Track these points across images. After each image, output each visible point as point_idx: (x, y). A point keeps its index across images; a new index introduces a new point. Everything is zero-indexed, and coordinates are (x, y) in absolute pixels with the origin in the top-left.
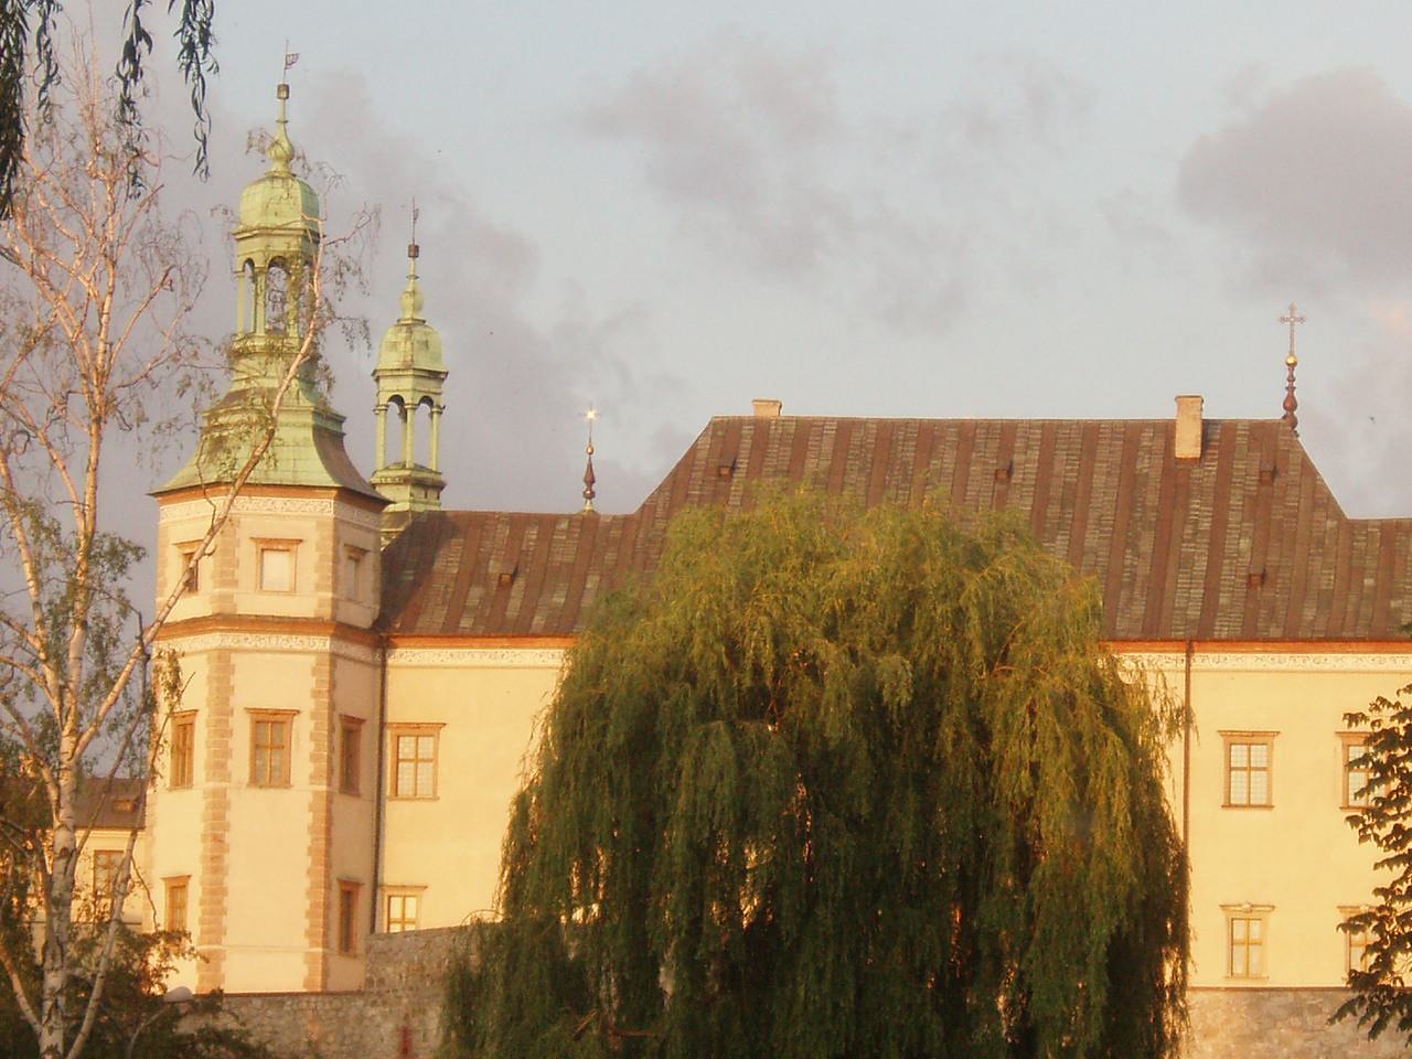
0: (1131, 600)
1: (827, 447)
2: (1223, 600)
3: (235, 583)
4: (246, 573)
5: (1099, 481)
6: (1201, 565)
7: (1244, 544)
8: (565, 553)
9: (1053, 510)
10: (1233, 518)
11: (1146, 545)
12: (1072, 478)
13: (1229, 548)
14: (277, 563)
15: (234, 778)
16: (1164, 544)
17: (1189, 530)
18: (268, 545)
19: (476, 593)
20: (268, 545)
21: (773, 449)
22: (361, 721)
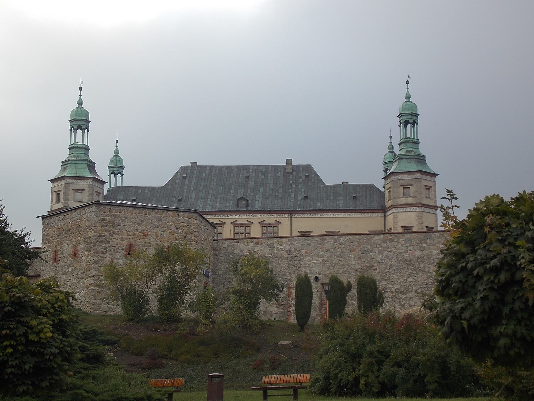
1: (207, 172)
3: (68, 200)
4: (71, 197)
5: (269, 178)
7: (303, 190)
10: (300, 185)
11: (280, 191)
12: (263, 177)
14: (79, 195)
17: (290, 188)
18: (77, 191)
20: (77, 191)
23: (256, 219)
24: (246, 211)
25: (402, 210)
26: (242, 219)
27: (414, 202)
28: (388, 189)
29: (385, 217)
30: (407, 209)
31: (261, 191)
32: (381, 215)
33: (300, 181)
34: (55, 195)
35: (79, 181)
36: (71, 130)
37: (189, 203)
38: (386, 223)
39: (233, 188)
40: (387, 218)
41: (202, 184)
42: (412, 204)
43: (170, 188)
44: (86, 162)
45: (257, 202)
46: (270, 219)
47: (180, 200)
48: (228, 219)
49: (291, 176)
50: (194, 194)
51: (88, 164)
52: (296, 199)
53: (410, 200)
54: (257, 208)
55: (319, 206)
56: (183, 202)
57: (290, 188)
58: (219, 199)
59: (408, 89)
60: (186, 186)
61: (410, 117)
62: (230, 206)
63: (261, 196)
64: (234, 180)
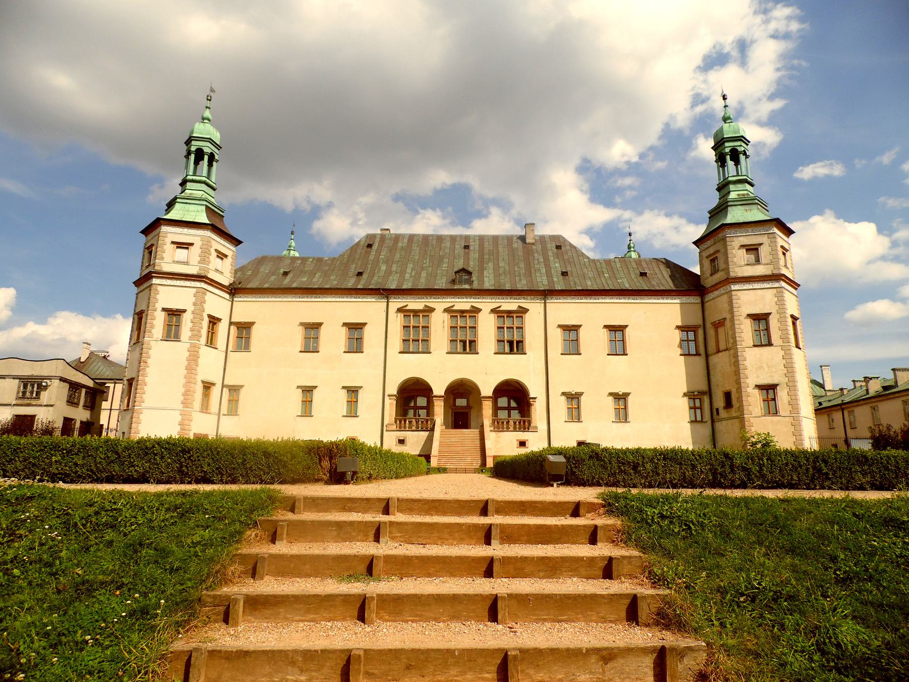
0: (520, 280)
1: (406, 241)
2: (555, 279)
5: (501, 249)
6: (544, 271)
7: (557, 265)
8: (309, 266)
9: (486, 257)
10: (551, 259)
11: (522, 265)
13: (552, 265)
14: (182, 254)
15: (155, 337)
16: (529, 266)
18: (181, 245)
19: (273, 278)
20: (181, 245)
21: (387, 242)
22: (219, 320)
23: (486, 305)
24: (471, 290)
25: (747, 286)
26: (463, 303)
27: (769, 272)
28: (707, 257)
29: (703, 304)
30: (756, 286)
31: (491, 265)
32: (695, 300)
33: (550, 254)
34: (147, 255)
35: (186, 230)
36: (187, 156)
37: (375, 278)
38: (707, 313)
39: (446, 260)
40: (707, 305)
41: (397, 256)
42: (766, 276)
43: (346, 260)
44: (205, 203)
45: (486, 279)
46: (510, 304)
47: (360, 274)
48: (439, 304)
49: (534, 247)
50: (384, 268)
51: (207, 206)
52: (549, 274)
53: (760, 270)
54: (488, 284)
55: (590, 285)
56: (365, 276)
57: (536, 262)
58: (424, 274)
59: (726, 106)
60: (372, 257)
61: (739, 143)
62: (442, 283)
63: (491, 271)
64: (447, 251)
